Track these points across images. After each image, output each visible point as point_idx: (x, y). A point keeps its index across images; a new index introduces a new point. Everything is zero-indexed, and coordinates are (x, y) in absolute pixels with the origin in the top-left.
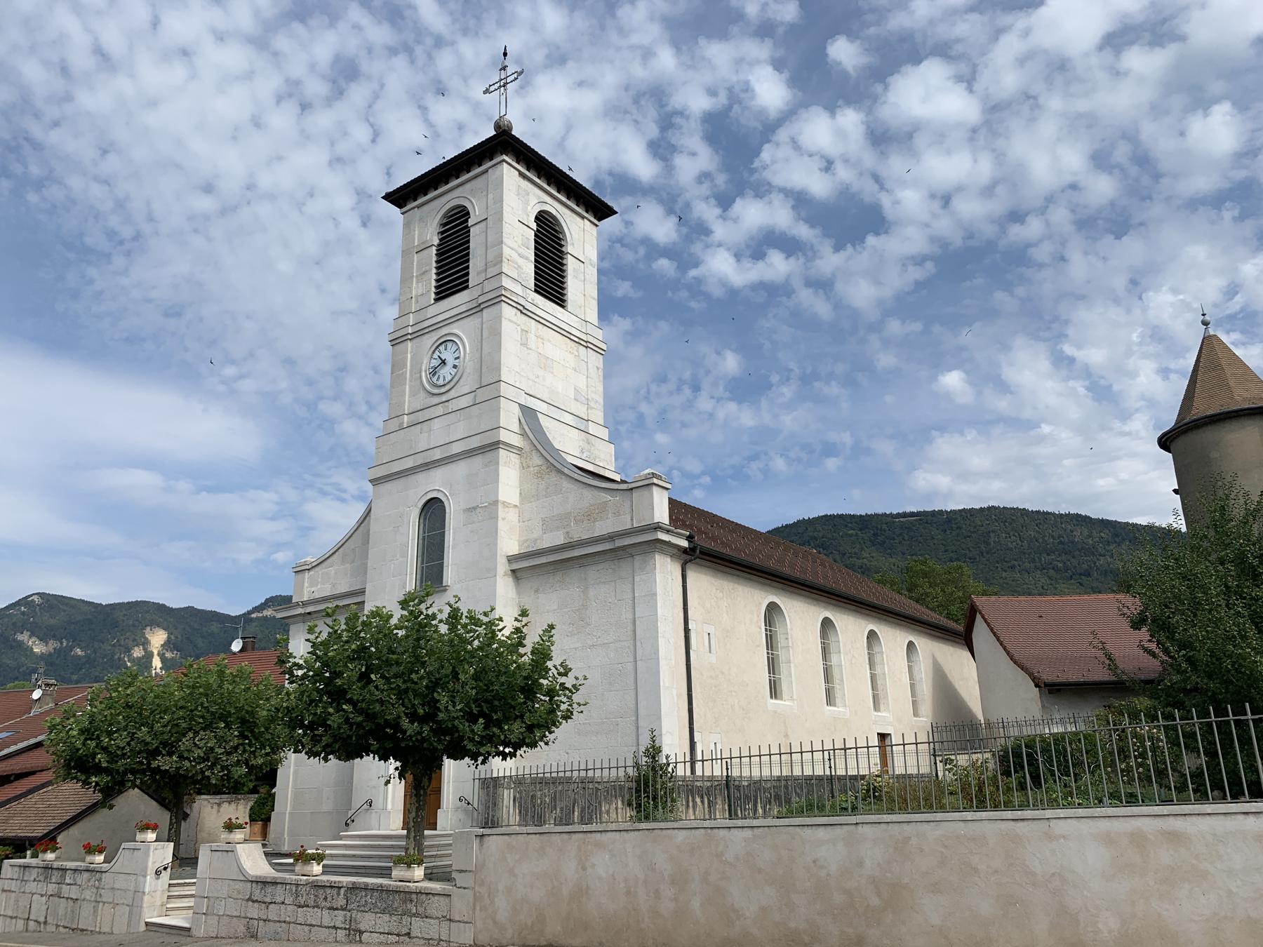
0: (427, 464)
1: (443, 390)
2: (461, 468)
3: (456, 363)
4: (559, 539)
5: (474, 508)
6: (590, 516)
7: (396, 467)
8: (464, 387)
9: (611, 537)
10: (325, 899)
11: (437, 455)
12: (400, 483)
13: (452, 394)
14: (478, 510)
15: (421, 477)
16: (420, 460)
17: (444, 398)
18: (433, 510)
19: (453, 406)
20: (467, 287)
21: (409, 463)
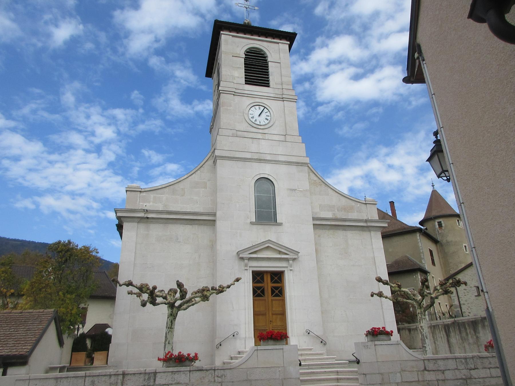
0: (260, 160)
1: (262, 127)
2: (283, 169)
3: (269, 118)
4: (329, 215)
5: (295, 190)
6: (345, 209)
7: (238, 155)
8: (272, 131)
9: (366, 221)
10: (490, 363)
11: (269, 158)
12: (240, 164)
13: (266, 131)
14: (297, 191)
15: (256, 165)
16: (256, 156)
17: (261, 131)
18: (265, 184)
19: (267, 136)
20: (268, 86)
21: (248, 156)
